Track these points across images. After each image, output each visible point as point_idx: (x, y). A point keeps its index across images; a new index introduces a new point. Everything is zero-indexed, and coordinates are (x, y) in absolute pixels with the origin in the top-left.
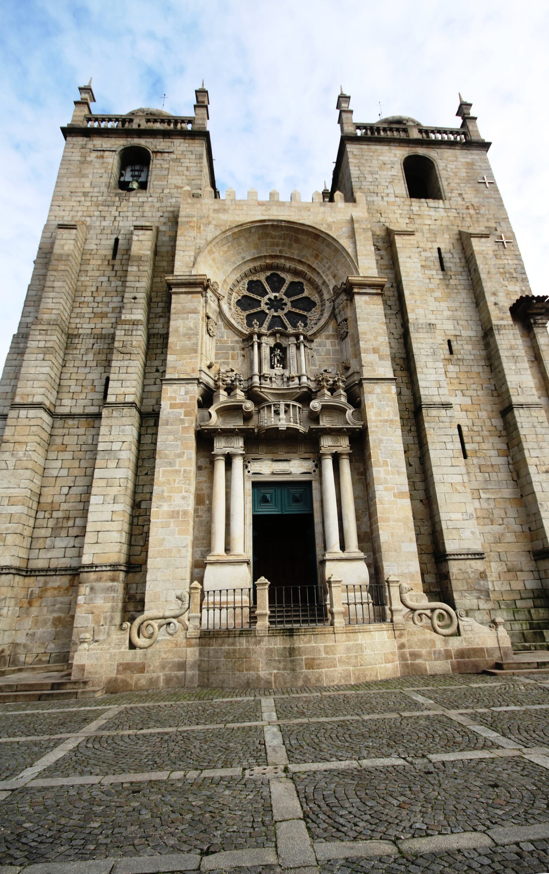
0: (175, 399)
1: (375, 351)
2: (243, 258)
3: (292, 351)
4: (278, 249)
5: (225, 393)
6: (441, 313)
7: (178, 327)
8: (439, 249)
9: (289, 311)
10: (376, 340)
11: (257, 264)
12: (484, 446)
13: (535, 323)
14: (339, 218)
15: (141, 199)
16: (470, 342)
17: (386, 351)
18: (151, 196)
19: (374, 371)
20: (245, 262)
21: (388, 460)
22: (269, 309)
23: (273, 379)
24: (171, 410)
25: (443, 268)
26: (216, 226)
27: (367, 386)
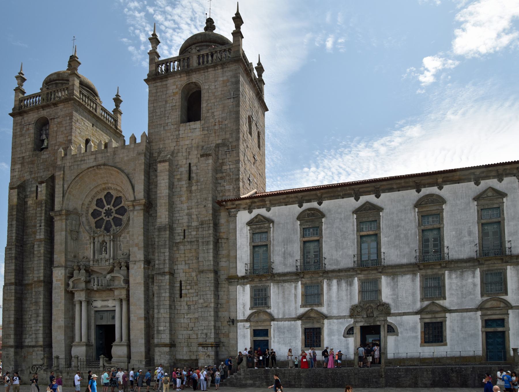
0: (57, 277)
1: (137, 245)
2: (90, 188)
3: (108, 244)
4: (105, 179)
5: (78, 272)
6: (183, 212)
8: (190, 164)
12: (191, 291)
13: (229, 214)
16: (195, 230)
17: (142, 244)
19: (136, 257)
20: (91, 190)
23: (100, 261)
25: (190, 179)
27: (131, 266)
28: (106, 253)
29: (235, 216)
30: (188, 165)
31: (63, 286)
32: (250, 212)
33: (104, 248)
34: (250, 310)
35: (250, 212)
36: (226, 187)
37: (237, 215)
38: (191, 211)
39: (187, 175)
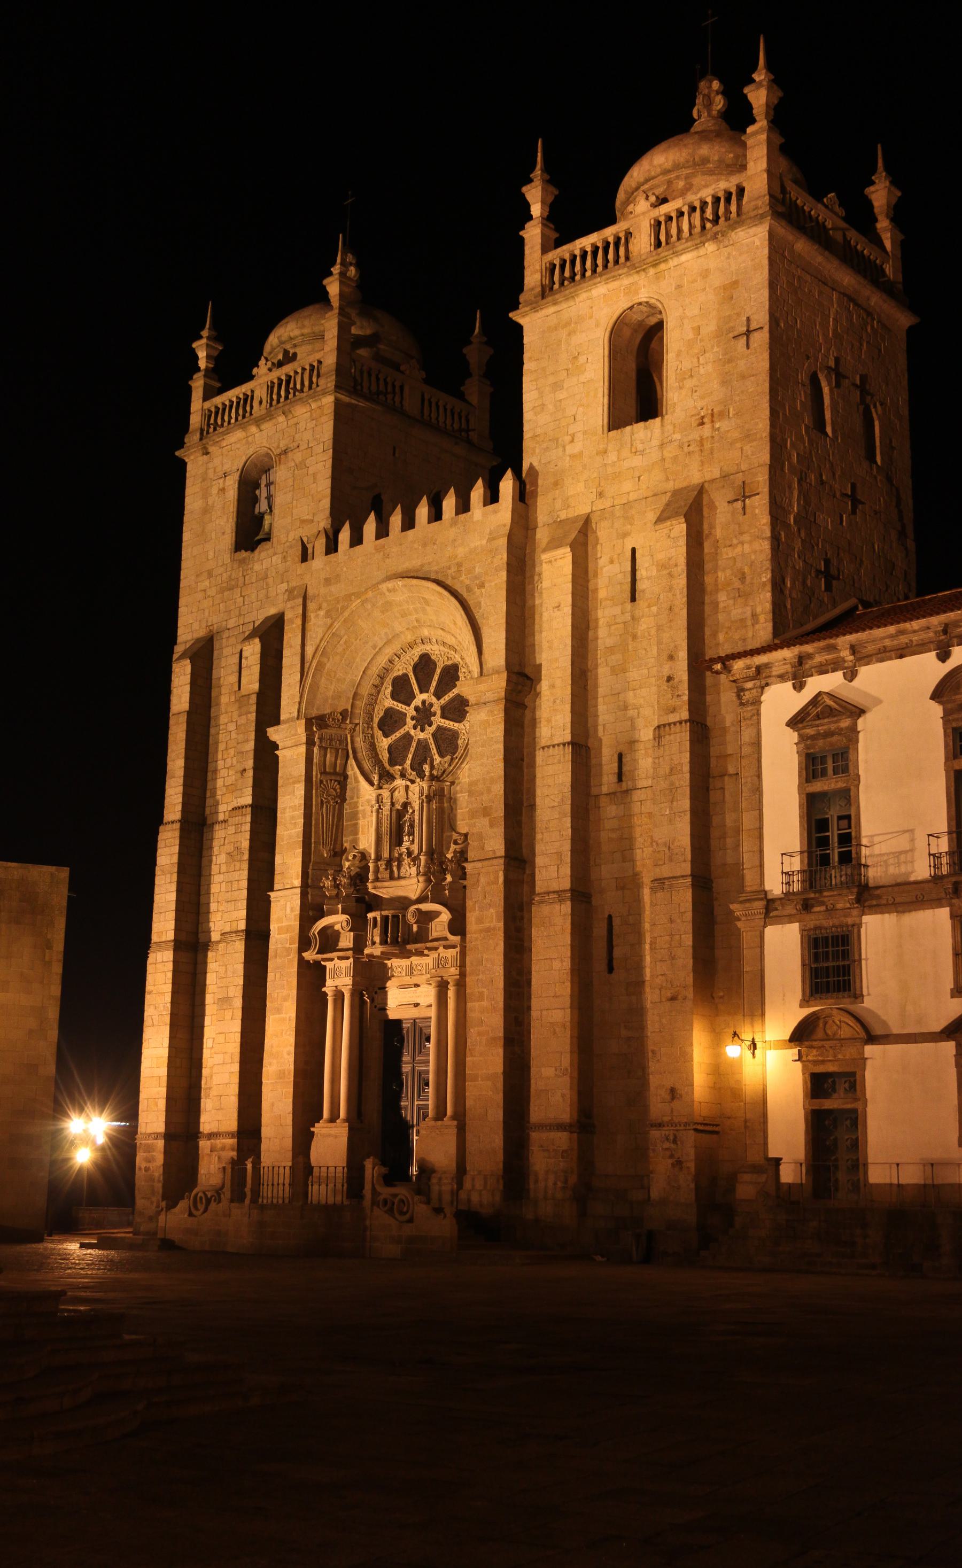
1: (486, 812)
2: (374, 647)
7: (285, 809)
8: (634, 551)
9: (439, 727)
10: (489, 791)
11: (395, 647)
14: (472, 545)
15: (266, 564)
17: (499, 810)
18: (275, 554)
20: (377, 652)
21: (485, 990)
22: (415, 728)
24: (279, 936)
26: (328, 612)
28: (413, 841)
29: (757, 702)
30: (629, 554)
31: (295, 946)
32: (799, 687)
33: (407, 824)
34: (801, 1006)
35: (799, 687)
36: (734, 612)
37: (763, 698)
38: (638, 691)
39: (628, 587)
